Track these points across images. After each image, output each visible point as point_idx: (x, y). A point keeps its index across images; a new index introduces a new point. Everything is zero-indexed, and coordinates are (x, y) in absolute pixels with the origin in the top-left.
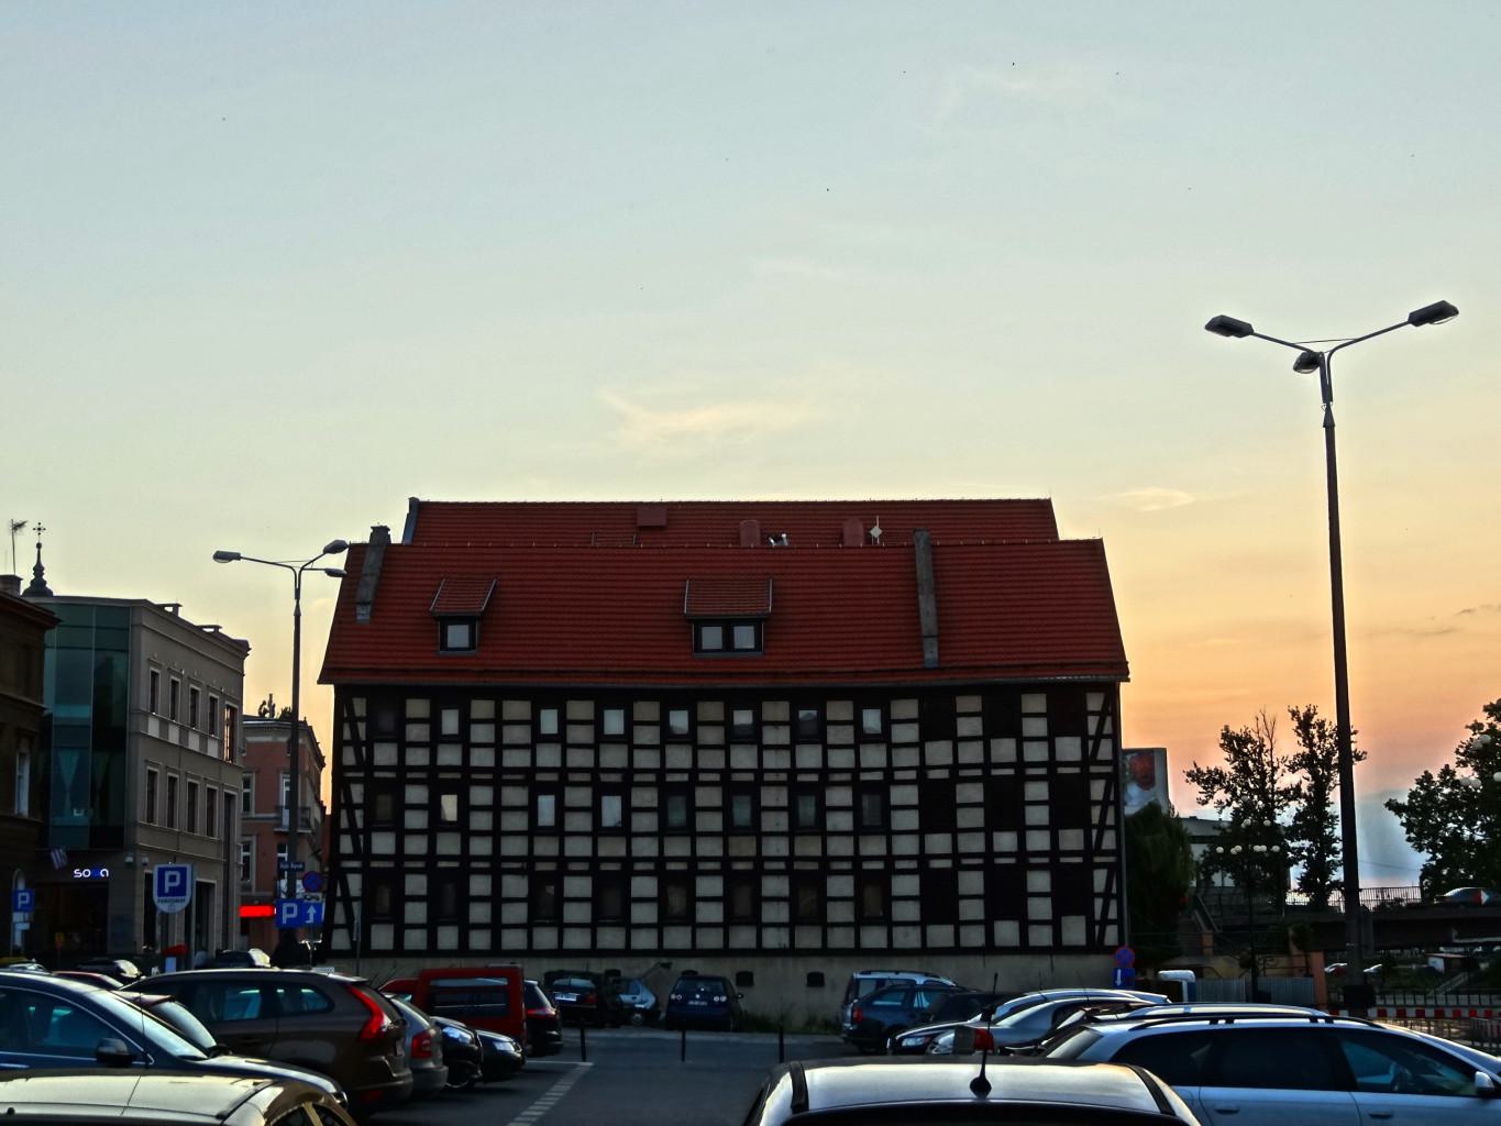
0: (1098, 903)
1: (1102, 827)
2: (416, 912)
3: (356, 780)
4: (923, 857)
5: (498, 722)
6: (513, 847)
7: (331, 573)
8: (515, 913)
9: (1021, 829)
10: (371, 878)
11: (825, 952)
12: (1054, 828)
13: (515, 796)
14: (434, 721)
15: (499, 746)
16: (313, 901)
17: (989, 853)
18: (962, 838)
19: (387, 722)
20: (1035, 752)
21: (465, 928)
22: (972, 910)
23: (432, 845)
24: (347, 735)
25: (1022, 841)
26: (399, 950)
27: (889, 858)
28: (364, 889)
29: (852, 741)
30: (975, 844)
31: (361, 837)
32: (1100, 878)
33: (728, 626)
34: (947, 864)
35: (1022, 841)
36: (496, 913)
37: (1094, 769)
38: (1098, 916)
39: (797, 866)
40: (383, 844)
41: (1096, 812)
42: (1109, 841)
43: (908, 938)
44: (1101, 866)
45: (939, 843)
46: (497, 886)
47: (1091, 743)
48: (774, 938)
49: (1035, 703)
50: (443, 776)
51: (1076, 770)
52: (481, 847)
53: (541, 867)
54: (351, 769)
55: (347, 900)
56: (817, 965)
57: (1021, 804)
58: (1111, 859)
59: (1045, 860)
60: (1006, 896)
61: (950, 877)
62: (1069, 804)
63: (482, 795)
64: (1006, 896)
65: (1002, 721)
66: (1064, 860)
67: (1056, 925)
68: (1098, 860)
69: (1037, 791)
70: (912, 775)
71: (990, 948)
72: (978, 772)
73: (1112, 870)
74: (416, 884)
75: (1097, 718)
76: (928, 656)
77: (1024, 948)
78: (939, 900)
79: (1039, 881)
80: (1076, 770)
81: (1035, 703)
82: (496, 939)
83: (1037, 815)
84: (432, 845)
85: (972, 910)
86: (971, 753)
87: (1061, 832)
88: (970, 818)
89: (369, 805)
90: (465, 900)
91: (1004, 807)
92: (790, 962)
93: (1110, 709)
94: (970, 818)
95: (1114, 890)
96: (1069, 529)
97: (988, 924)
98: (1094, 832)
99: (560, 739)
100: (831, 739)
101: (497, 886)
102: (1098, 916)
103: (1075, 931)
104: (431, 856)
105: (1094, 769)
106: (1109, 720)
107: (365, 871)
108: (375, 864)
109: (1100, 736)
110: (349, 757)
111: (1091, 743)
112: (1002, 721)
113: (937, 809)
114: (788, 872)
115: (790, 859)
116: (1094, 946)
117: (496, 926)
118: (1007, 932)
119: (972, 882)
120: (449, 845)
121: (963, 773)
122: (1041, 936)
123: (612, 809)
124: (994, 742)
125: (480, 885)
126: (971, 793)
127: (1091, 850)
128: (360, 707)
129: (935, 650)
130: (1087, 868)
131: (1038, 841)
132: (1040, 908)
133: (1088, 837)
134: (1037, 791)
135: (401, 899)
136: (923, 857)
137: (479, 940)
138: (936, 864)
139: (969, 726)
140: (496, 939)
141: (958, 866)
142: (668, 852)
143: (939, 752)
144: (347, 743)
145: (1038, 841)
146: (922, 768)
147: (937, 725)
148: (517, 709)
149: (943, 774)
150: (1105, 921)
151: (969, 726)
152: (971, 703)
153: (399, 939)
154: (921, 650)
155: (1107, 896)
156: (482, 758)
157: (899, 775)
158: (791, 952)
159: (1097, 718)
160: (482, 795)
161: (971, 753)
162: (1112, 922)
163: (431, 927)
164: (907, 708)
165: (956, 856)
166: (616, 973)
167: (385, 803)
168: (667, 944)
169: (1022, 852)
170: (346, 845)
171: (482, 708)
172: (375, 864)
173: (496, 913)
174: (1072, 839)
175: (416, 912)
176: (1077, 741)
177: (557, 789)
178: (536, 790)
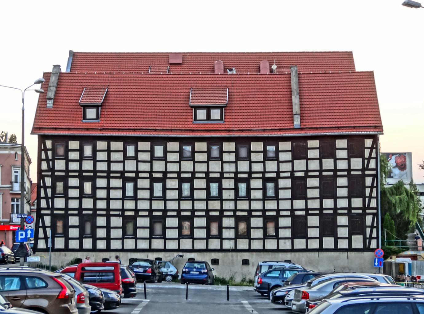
1: (370, 197)
2: (74, 233)
3: (47, 176)
4: (292, 210)
5: (109, 151)
6: (116, 205)
7: (37, 91)
8: (116, 233)
9: (335, 198)
10: (55, 218)
11: (250, 250)
12: (349, 198)
13: (116, 183)
14: (81, 150)
15: (109, 161)
16: (30, 228)
17: (321, 209)
18: (309, 201)
19: (61, 151)
20: (343, 165)
21: (95, 240)
22: (313, 233)
23: (81, 203)
24: (43, 157)
25: (335, 203)
26: (67, 249)
27: (278, 211)
28: (51, 223)
29: (262, 160)
30: (315, 204)
32: (369, 220)
33: (209, 109)
34: (303, 213)
35: (335, 203)
36: (108, 233)
37: (367, 172)
38: (368, 236)
39: (238, 213)
40: (59, 203)
41: (368, 191)
42: (373, 203)
43: (286, 245)
45: (299, 204)
46: (108, 221)
47: (366, 161)
48: (228, 245)
49: (342, 143)
50: (84, 174)
51: (360, 173)
52: (102, 205)
53: (127, 213)
54: (45, 171)
55: (44, 227)
56: (246, 256)
57: (335, 187)
58: (375, 211)
59: (346, 212)
60: (328, 227)
61: (305, 218)
62: (356, 187)
63: (102, 183)
64: (328, 227)
66: (353, 211)
68: (368, 211)
69: (342, 181)
70: (288, 175)
71: (321, 249)
72: (317, 174)
73: (375, 215)
74: (74, 221)
75: (369, 150)
76: (295, 123)
77: (336, 249)
78: (299, 229)
79: (343, 220)
80: (360, 173)
81: (342, 143)
82: (108, 244)
83: (342, 192)
84: (81, 203)
85: (313, 233)
86: (314, 165)
87: (352, 199)
88: (314, 193)
89: (53, 187)
90: (94, 227)
91: (328, 189)
92: (235, 254)
93: (375, 146)
94: (314, 193)
95: (375, 225)
96: (360, 66)
97: (321, 239)
98: (367, 200)
99: (136, 158)
100: (253, 159)
101: (108, 221)
102: (368, 236)
103: (358, 242)
104: (80, 209)
105: (367, 172)
106: (374, 151)
107: (53, 216)
108: (55, 212)
109: (370, 158)
110: (44, 166)
111: (366, 161)
112: (328, 151)
113: (299, 189)
115: (235, 211)
116: (366, 249)
117: (108, 239)
118: (328, 242)
119: (313, 221)
120: (88, 203)
121: (310, 174)
122: (343, 244)
123: (158, 188)
124: (323, 160)
125: (101, 221)
126: (313, 182)
128: (49, 144)
129: (299, 120)
130: (364, 214)
131: (343, 203)
132: (343, 232)
133: (364, 202)
134: (342, 181)
135: (66, 227)
136: (292, 210)
137: (101, 245)
138: (297, 213)
139: (313, 154)
140: (108, 244)
141: (308, 214)
142: (182, 207)
143: (300, 165)
144: (44, 160)
145: (343, 203)
146: (293, 172)
147: (299, 153)
148: (117, 145)
149: (302, 174)
150: (371, 238)
151: (313, 154)
152: (315, 143)
153: (67, 244)
154: (293, 120)
155: (372, 227)
157: (282, 175)
158: (235, 250)
159: (369, 150)
160: (102, 183)
161: (314, 165)
162: (374, 238)
163: (80, 239)
164: (286, 146)
165: (307, 210)
166: (160, 259)
167: (60, 186)
168: (182, 247)
169: (335, 209)
170: (43, 204)
171: (102, 145)
172: (55, 212)
173: (108, 233)
174: (357, 202)
175: (74, 233)
176: (360, 160)
177: (134, 180)
178: (126, 180)
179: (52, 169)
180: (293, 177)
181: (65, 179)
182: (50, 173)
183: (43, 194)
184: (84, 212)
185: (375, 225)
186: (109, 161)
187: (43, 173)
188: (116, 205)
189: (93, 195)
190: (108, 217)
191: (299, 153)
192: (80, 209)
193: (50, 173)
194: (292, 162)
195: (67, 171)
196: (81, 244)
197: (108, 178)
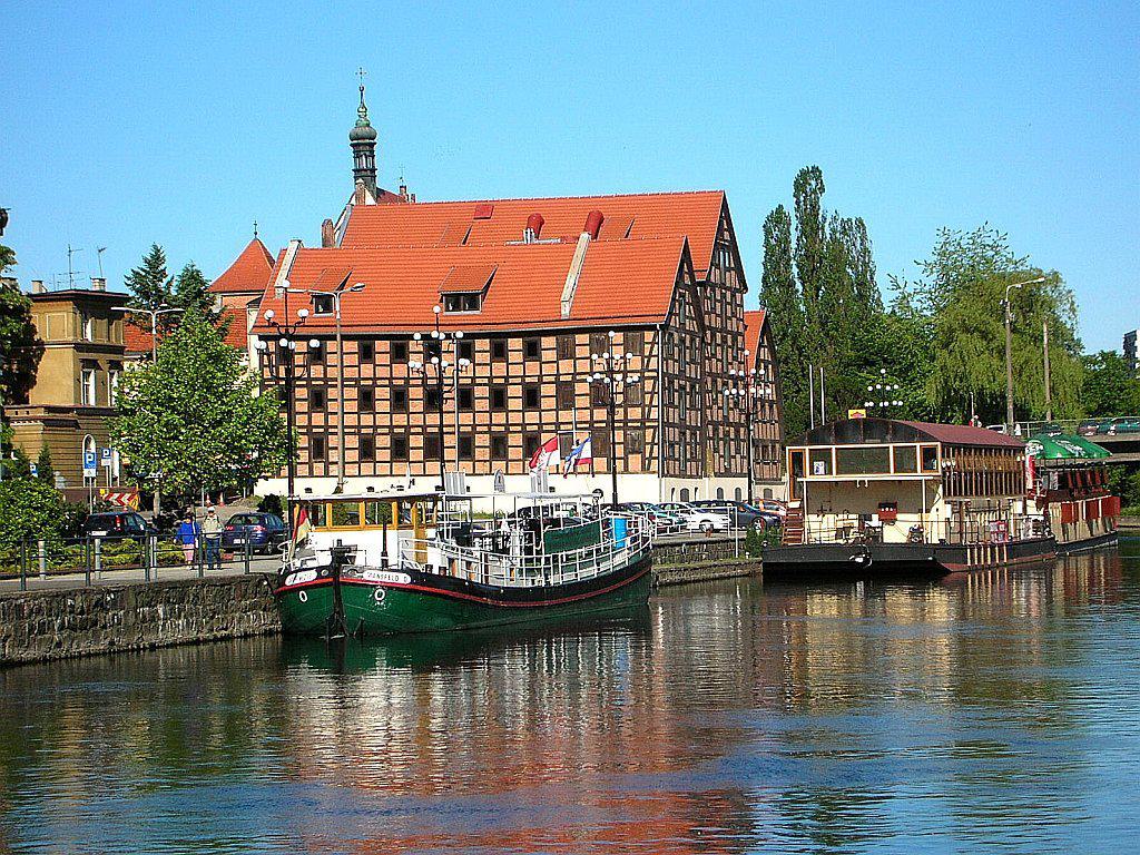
0: (648, 447)
6: (351, 420)
24: (266, 363)
37: (646, 374)
39: (494, 429)
42: (654, 414)
44: (649, 427)
54: (268, 380)
65: (600, 346)
67: (626, 459)
70: (553, 379)
76: (563, 312)
102: (647, 456)
104: (310, 426)
109: (651, 356)
112: (600, 346)
114: (489, 432)
116: (645, 469)
127: (644, 420)
139: (582, 352)
143: (566, 366)
148: (353, 346)
149: (569, 378)
152: (583, 338)
162: (655, 458)
180: (557, 382)
184: (314, 430)
185: (656, 441)
191: (565, 352)
192: (310, 426)
194: (523, 363)
196: (311, 470)
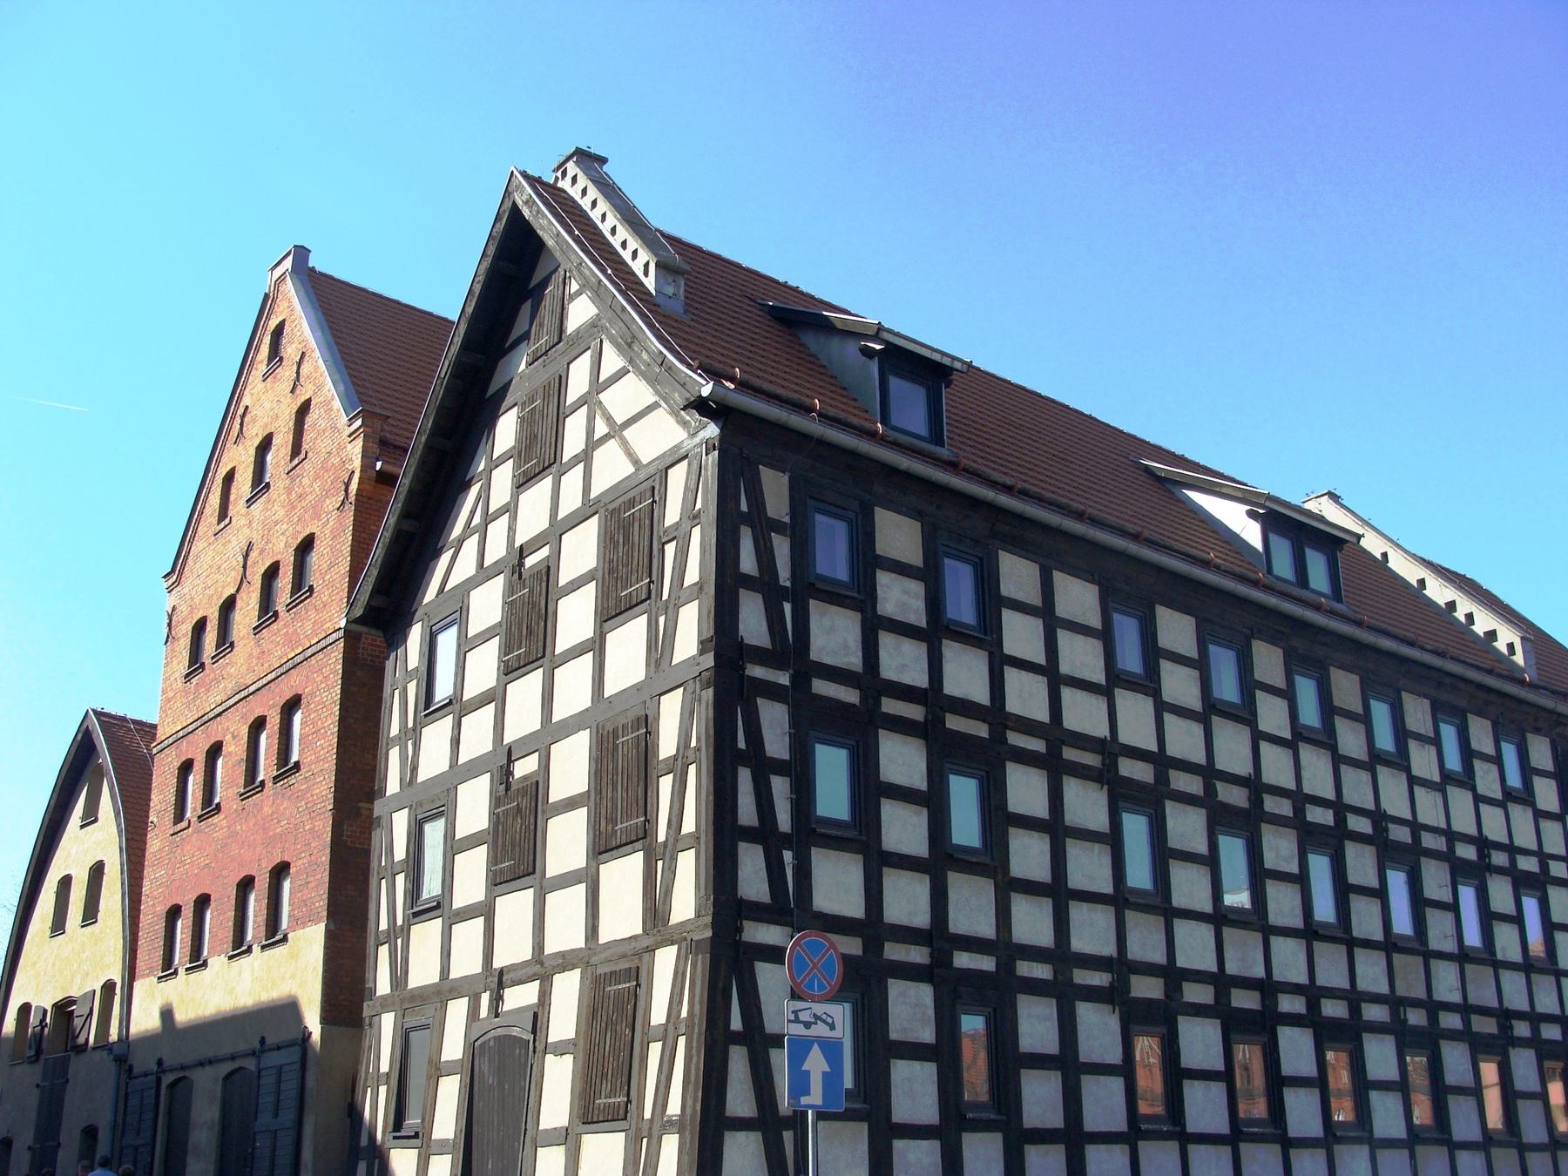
3: (773, 692)
31: (788, 856)
104: (938, 936)
120: (972, 909)
156: (1026, 696)
160: (1026, 790)
167: (832, 768)
171: (1017, 575)
179: (791, 648)
181: (858, 729)
182: (784, 679)
183: (747, 812)
184: (963, 960)
186: (1050, 671)
187: (757, 671)
188: (1092, 932)
189: (989, 861)
190: (1065, 996)
193: (784, 679)
195: (869, 678)
197: (1055, 768)
